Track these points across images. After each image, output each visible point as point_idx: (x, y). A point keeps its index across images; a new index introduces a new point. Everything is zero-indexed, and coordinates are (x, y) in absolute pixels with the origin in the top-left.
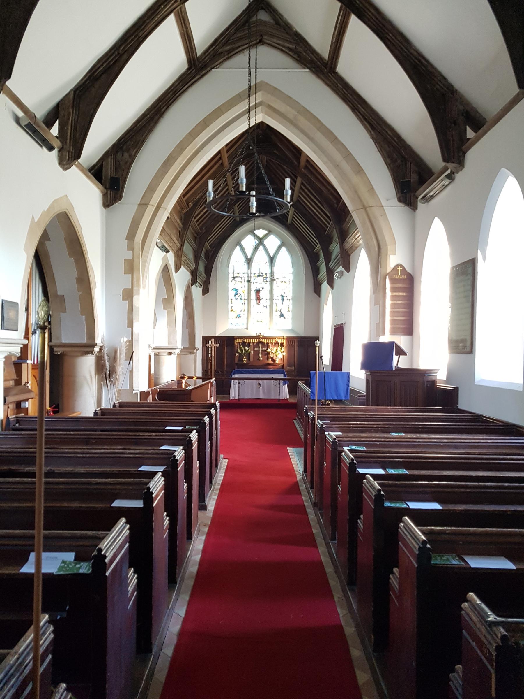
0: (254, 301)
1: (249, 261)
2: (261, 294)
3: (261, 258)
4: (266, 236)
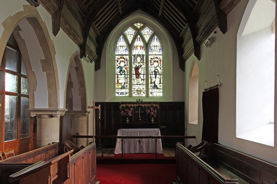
0: (134, 77)
1: (130, 47)
2: (140, 70)
3: (139, 43)
4: (142, 28)
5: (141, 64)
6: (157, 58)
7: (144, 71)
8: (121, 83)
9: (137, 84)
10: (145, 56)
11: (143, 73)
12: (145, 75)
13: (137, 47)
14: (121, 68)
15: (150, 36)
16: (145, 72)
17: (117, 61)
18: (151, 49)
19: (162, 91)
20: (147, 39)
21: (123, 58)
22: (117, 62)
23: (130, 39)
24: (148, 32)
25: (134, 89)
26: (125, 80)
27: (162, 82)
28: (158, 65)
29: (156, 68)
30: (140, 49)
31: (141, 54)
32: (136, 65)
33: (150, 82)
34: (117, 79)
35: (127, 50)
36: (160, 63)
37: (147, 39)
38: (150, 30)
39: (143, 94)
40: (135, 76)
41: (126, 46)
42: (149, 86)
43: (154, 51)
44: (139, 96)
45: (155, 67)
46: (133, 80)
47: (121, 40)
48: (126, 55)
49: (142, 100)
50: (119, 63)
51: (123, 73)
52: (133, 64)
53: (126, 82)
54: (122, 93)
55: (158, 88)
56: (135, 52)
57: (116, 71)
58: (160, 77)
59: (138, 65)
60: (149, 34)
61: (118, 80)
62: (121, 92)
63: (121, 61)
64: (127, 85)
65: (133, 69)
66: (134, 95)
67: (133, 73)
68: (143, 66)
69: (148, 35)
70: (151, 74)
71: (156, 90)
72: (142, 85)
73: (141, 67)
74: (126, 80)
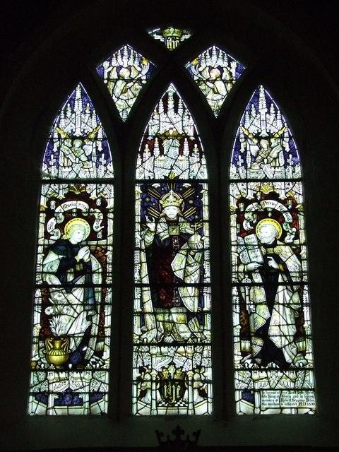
0: (144, 299)
1: (125, 138)
2: (178, 263)
3: (171, 119)
4: (191, 50)
5: (187, 228)
6: (273, 196)
7: (202, 270)
8: (67, 337)
9: (162, 344)
10: (205, 186)
11: (194, 279)
12: (207, 290)
13: (161, 142)
14: (66, 249)
15: (229, 87)
16: (208, 274)
17: (50, 214)
18: (238, 148)
19: (310, 378)
20: (216, 97)
21: (85, 197)
22: (47, 220)
23: (124, 103)
24: (220, 68)
25: (142, 370)
26: (89, 318)
27: (308, 332)
28: (285, 233)
29: (270, 250)
30: (181, 153)
31: (185, 176)
32: (157, 236)
33: (237, 332)
34: (43, 314)
35: (107, 158)
36: (294, 223)
37: (216, 97)
38: (230, 61)
39: (197, 398)
40: (147, 296)
41: (100, 136)
42: (232, 355)
44: (172, 411)
45: (266, 246)
47: (73, 106)
48: (98, 181)
49: (197, 434)
50: (61, 227)
51: (81, 281)
52: (138, 227)
53: (95, 330)
54: (69, 397)
55: (285, 367)
56: (148, 167)
57: (39, 269)
58: (296, 298)
59: (163, 231)
60: (226, 76)
62: (62, 388)
63: (70, 212)
64: (101, 344)
65: (140, 257)
66: (140, 408)
67: (136, 276)
68: (195, 239)
69: (220, 85)
70: (239, 285)
71: (274, 376)
72: (190, 350)
73: (185, 246)
74: (96, 319)
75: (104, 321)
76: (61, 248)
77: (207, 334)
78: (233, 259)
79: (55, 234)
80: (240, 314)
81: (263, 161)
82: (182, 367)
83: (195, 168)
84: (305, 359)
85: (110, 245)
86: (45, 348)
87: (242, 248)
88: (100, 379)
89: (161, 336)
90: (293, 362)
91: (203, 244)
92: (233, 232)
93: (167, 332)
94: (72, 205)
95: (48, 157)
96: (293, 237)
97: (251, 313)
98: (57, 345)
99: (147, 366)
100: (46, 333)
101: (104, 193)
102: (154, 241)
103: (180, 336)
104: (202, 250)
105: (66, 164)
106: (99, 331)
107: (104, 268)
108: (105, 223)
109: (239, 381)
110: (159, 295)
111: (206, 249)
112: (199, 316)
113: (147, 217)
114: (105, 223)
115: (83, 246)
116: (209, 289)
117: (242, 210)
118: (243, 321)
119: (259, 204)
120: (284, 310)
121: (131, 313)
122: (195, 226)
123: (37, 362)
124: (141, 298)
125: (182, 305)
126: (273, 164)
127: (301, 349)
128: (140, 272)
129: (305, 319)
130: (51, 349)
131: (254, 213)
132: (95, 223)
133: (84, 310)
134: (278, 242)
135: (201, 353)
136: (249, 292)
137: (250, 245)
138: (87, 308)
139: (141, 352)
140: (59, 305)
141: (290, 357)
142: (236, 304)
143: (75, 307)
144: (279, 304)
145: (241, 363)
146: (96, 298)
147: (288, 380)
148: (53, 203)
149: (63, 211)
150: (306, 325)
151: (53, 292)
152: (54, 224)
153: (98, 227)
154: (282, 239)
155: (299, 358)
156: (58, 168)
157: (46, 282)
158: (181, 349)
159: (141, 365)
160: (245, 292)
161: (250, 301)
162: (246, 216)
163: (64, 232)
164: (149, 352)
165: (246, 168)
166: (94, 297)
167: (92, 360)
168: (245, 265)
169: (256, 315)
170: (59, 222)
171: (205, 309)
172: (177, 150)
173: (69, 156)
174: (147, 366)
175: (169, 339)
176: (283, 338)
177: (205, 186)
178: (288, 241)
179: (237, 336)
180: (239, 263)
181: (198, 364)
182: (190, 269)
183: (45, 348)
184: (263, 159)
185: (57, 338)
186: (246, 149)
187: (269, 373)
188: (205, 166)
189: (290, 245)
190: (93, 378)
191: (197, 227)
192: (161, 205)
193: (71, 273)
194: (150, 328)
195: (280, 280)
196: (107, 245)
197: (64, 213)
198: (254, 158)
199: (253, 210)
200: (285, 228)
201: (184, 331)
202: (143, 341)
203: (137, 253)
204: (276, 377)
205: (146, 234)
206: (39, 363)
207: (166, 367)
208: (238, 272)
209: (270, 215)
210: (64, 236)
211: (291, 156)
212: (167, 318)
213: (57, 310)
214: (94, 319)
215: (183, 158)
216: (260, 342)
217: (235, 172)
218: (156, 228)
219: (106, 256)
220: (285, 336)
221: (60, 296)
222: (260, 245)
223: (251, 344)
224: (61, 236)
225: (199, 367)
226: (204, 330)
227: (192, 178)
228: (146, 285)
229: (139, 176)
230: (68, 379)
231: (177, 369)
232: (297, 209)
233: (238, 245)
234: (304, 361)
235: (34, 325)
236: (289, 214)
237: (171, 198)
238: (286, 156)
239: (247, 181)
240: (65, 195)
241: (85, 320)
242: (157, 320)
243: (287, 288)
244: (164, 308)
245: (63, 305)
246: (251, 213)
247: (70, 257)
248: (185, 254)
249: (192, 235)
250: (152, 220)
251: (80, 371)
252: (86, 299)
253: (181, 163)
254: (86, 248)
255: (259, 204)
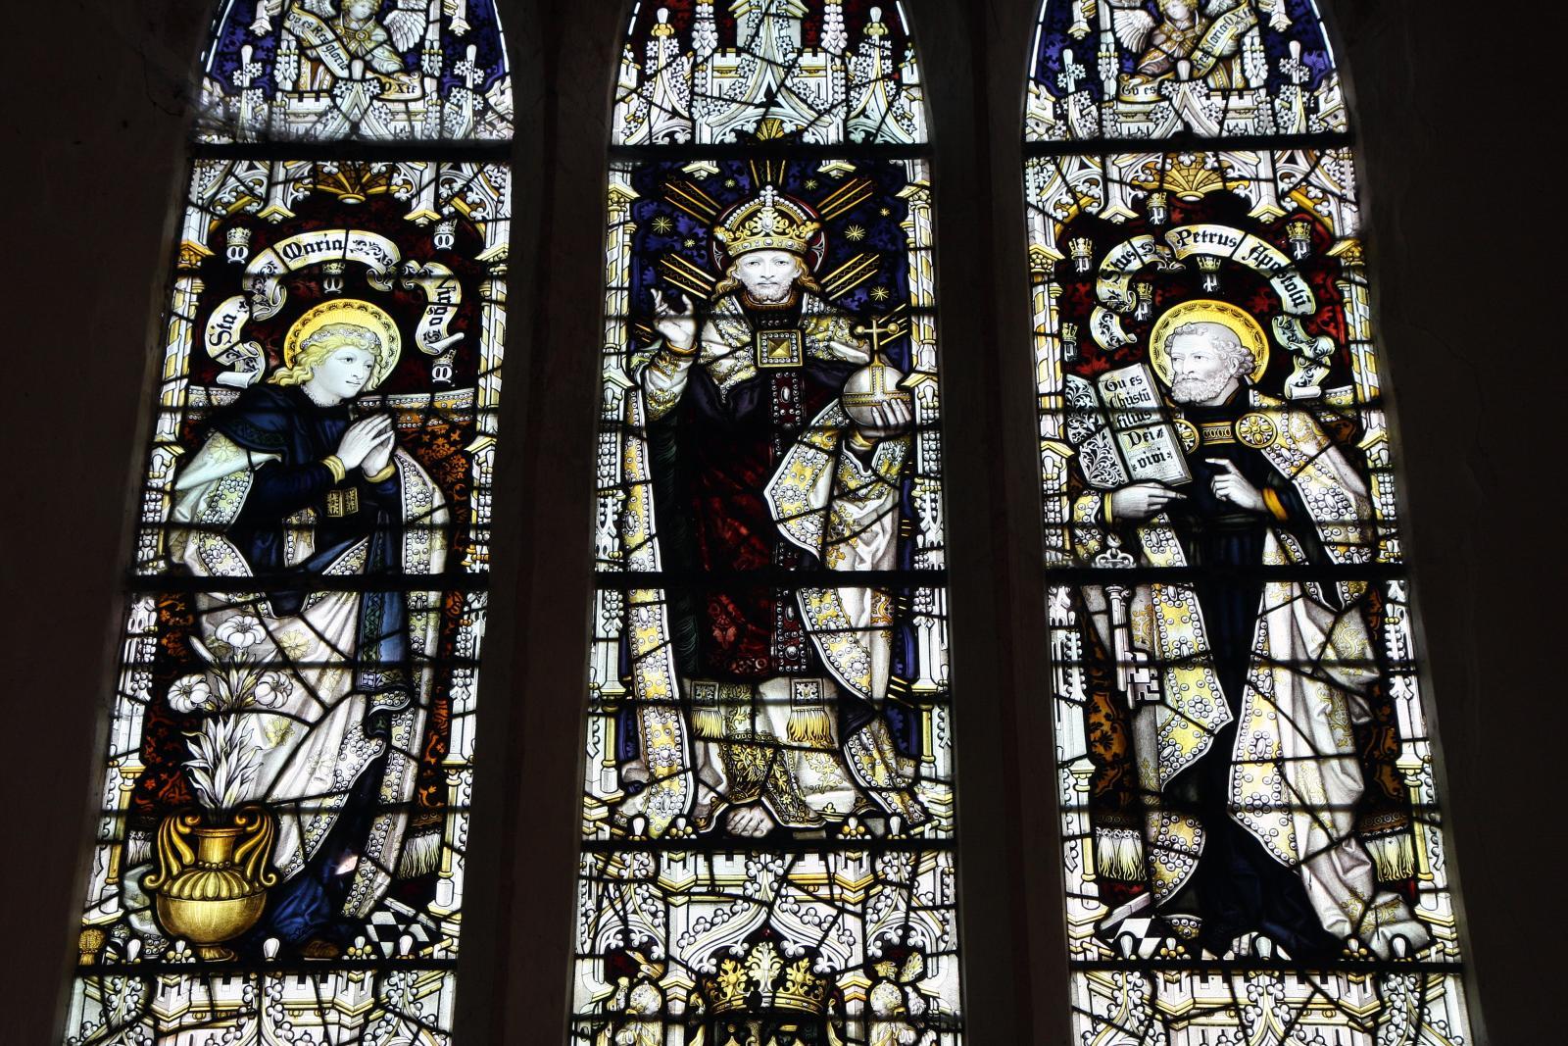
0: (636, 643)
2: (796, 487)
5: (836, 339)
6: (1227, 208)
7: (907, 515)
8: (266, 810)
9: (718, 841)
11: (873, 551)
12: (933, 602)
14: (289, 429)
16: (933, 533)
17: (222, 279)
21: (386, 216)
22: (207, 305)
25: (618, 965)
26: (375, 726)
27: (1423, 793)
28: (1282, 362)
29: (1219, 432)
30: (811, 38)
31: (830, 132)
33: (1074, 788)
35: (487, 61)
36: (1327, 317)
40: (652, 629)
42: (1058, 895)
43: (1153, 60)
45: (1198, 413)
46: (601, 735)
48: (444, 151)
50: (268, 334)
51: (349, 561)
52: (616, 336)
53: (401, 780)
55: (1317, 954)
57: (157, 509)
58: (1352, 638)
61: (170, 736)
63: (317, 272)
64: (425, 845)
67: (605, 539)
68: (876, 384)
70: (1080, 577)
72: (851, 873)
73: (828, 414)
74: (407, 732)
75: (446, 740)
76: (266, 421)
77: (935, 797)
78: (1049, 471)
79: (240, 365)
80: (1089, 708)
81: (1173, 68)
82: (813, 954)
83: (874, 100)
84: (1414, 917)
85: (486, 411)
86: (153, 863)
87: (1090, 423)
88: (411, 1010)
89: (713, 806)
90: (1356, 933)
91: (910, 405)
92: (1047, 355)
93: (742, 789)
94: (321, 246)
95: (229, 60)
96: (1320, 374)
97: (1142, 704)
98: (215, 849)
99: (645, 949)
100: (167, 792)
101: (472, 197)
102: (686, 392)
103: (804, 806)
104: (908, 432)
105: (305, 82)
106: (420, 782)
107: (457, 505)
108: (468, 320)
109: (1096, 1019)
110: (705, 627)
111: (924, 428)
112: (893, 713)
113: (658, 296)
114: (468, 320)
115: (365, 414)
116: (942, 595)
117: (1083, 267)
118: (1105, 741)
119: (1160, 241)
120: (1297, 692)
121: (575, 701)
122: (875, 331)
123: (106, 930)
124: (625, 639)
125: (816, 669)
126: (1219, 79)
127: (1395, 874)
128: (621, 524)
129: (1405, 732)
130: (184, 868)
131: (1136, 278)
132: (427, 318)
133: (355, 691)
134: (1255, 398)
135: (908, 886)
136: (1128, 613)
137: (1124, 410)
138: (368, 679)
139: (619, 881)
140: (239, 667)
141: (1343, 907)
142: (1067, 664)
143: (311, 676)
144: (1271, 663)
145: (1099, 934)
146: (417, 634)
147: (1341, 1018)
148: (238, 236)
149: (280, 270)
150: (1410, 758)
151: (211, 611)
152: (237, 326)
153: (437, 336)
154: (1272, 384)
155: (1385, 915)
156: (269, 98)
157: (184, 567)
158: (811, 867)
159: (616, 942)
160: (1108, 612)
161: (1132, 649)
162: (1104, 289)
163: (280, 355)
164: (653, 879)
165: (1098, 97)
166: (404, 631)
167: (383, 918)
168: (1102, 492)
169: (1163, 715)
170: (261, 313)
171: (924, 684)
172: (794, 31)
173: (322, 52)
174: (645, 949)
175: (752, 821)
176: (1302, 820)
177: (919, 173)
178: (1299, 393)
179: (1079, 809)
180: (1077, 486)
181: (894, 937)
182: (851, 512)
183: (153, 863)
184: (1172, 63)
185: (219, 817)
186: (1094, 22)
187: (1239, 983)
188: (916, 93)
189: (1310, 407)
190: (378, 1004)
191: (881, 336)
192: (722, 246)
193: (301, 528)
194: (661, 770)
195: (1271, 555)
196: (474, 410)
197: (288, 280)
198: (1130, 61)
199: (1135, 265)
200: (1282, 339)
201: (824, 787)
202: (630, 829)
203: (609, 443)
204: (1280, 1002)
205: (652, 365)
206: (119, 934)
207: (739, 949)
208: (1071, 525)
209: (1210, 284)
210: (281, 372)
211: (1295, 47)
212: (742, 726)
213: (224, 691)
214: (399, 731)
215: (821, 59)
216: (1186, 835)
217: (1049, 115)
218: (697, 337)
219: (470, 457)
220: (1311, 810)
221: (244, 629)
222: (1170, 408)
223: (1148, 845)
224: (269, 372)
225: (898, 953)
226: (918, 778)
227: (858, 137)
228: (646, 580)
229: (625, 129)
230: (256, 1014)
231: (789, 961)
232: (1337, 258)
233: (1069, 410)
234: (1413, 930)
235: (109, 761)
236: (1298, 281)
237: (768, 219)
238: (1274, 45)
239: (1101, 146)
240: (296, 205)
241: (358, 734)
242: (695, 735)
243: (1305, 595)
244: (727, 679)
245: (258, 668)
246: (1125, 281)
247: (301, 458)
248: (830, 445)
249: (858, 367)
250: (680, 308)
251: (319, 972)
252: (366, 639)
253: (812, 82)
254: (379, 422)
255: (1160, 241)
